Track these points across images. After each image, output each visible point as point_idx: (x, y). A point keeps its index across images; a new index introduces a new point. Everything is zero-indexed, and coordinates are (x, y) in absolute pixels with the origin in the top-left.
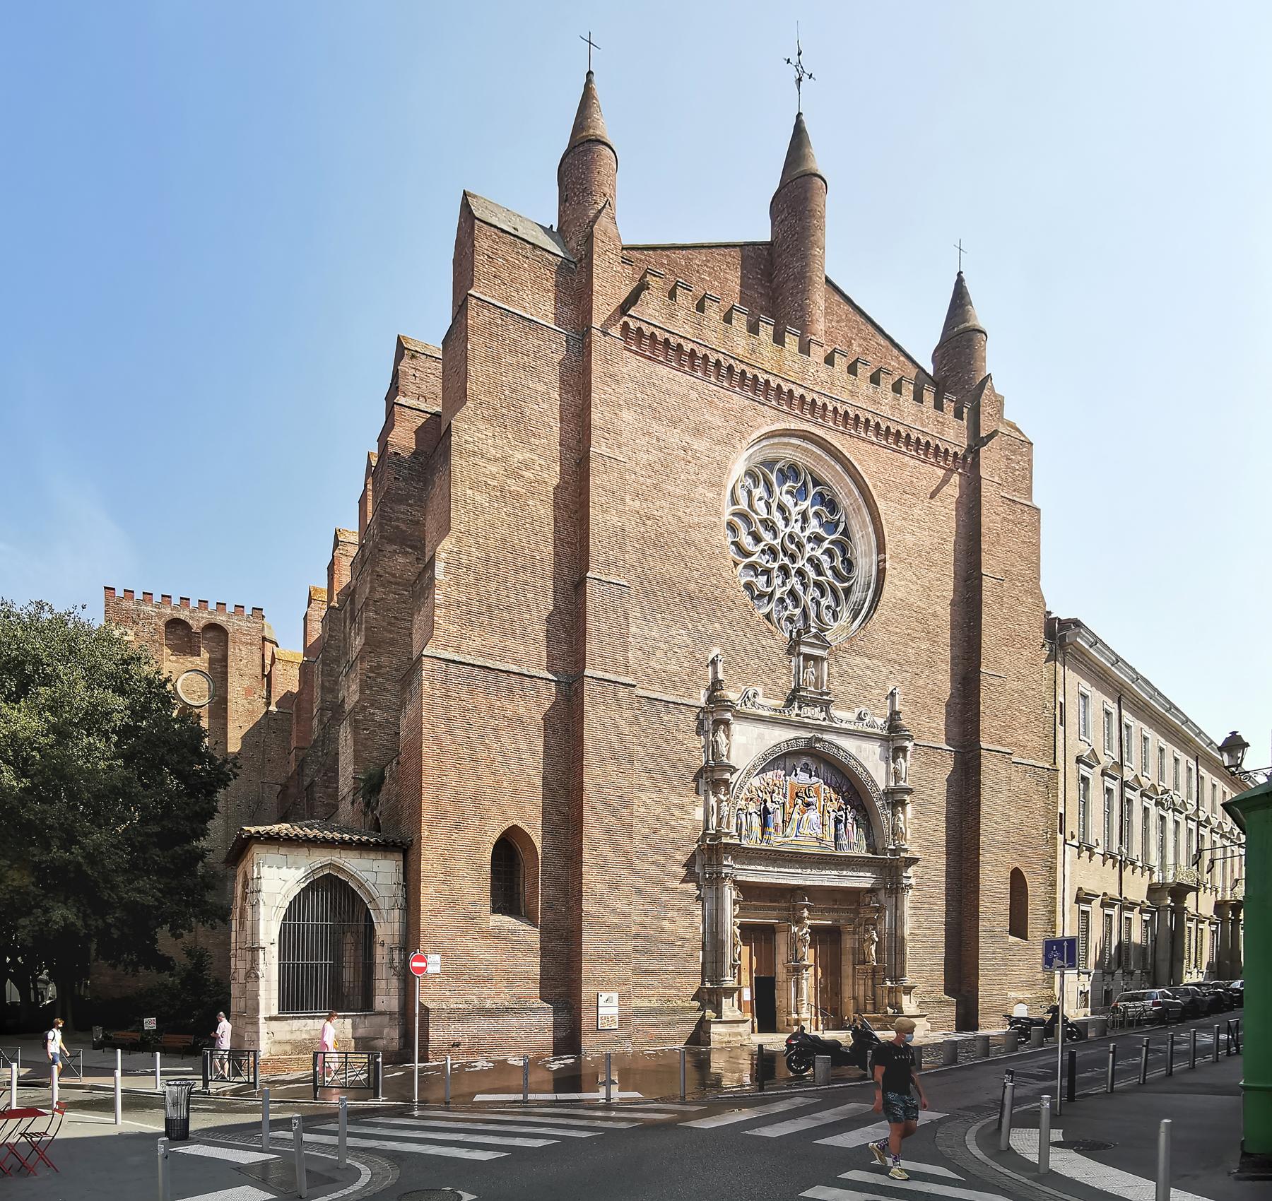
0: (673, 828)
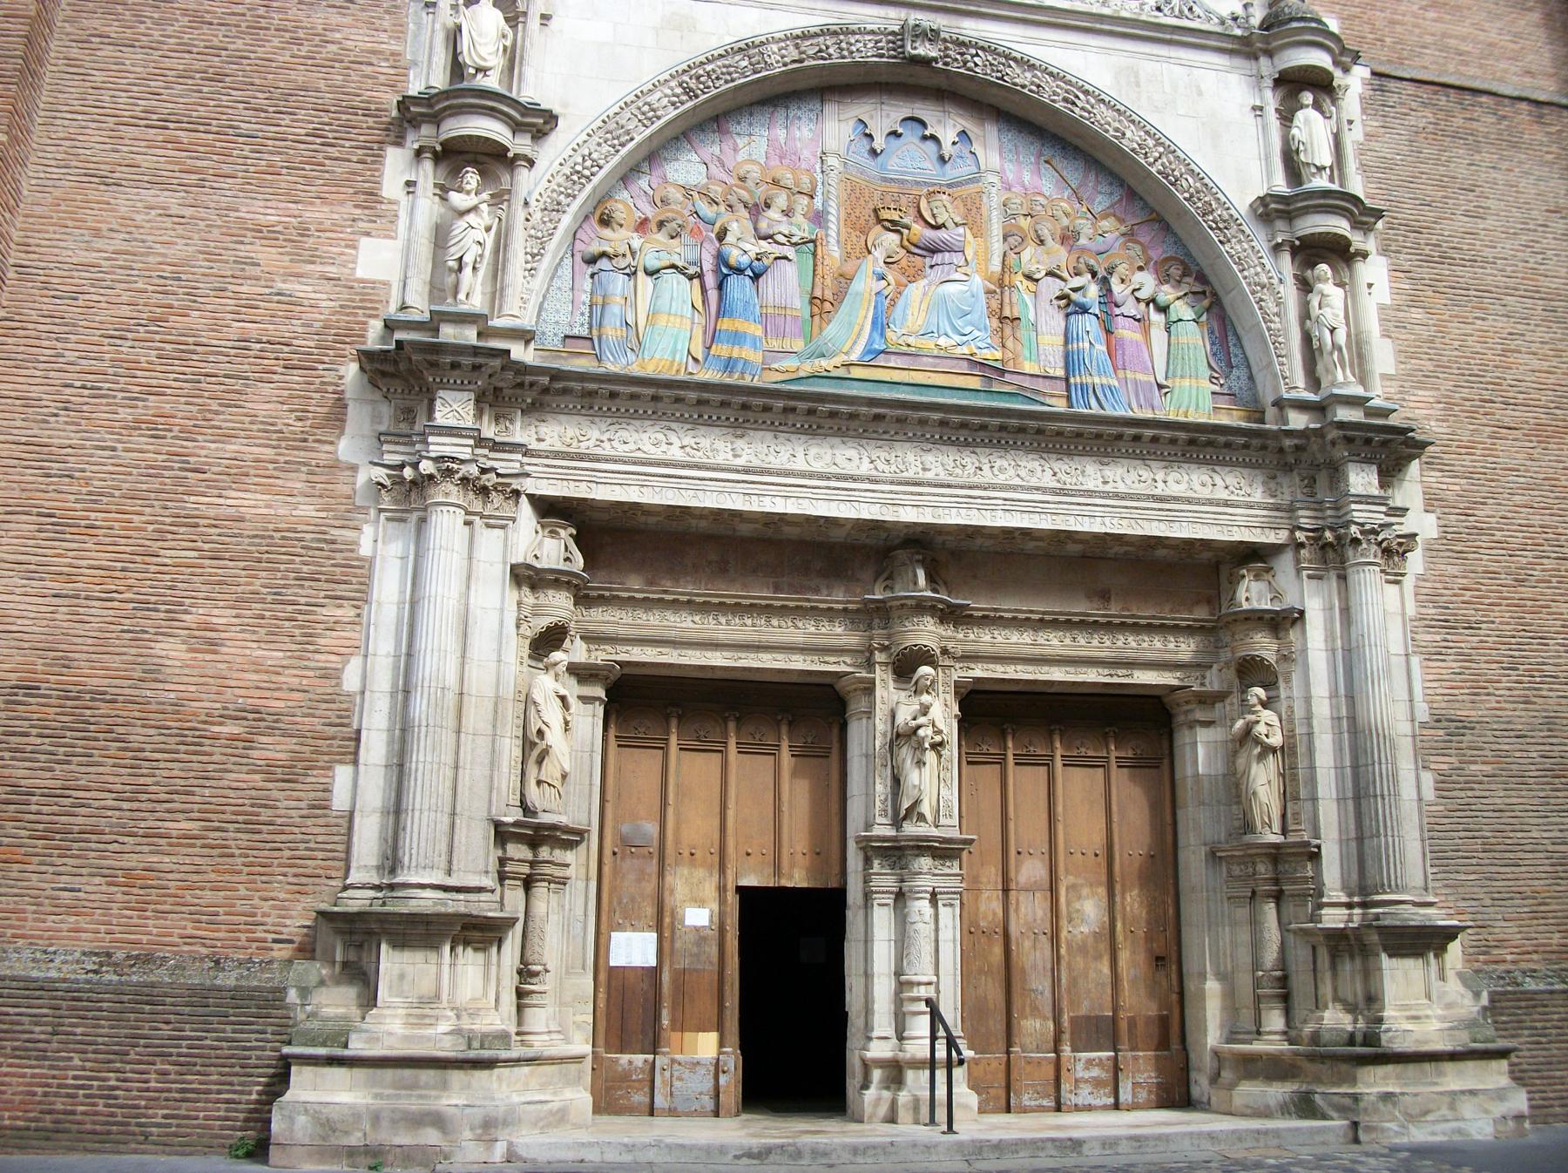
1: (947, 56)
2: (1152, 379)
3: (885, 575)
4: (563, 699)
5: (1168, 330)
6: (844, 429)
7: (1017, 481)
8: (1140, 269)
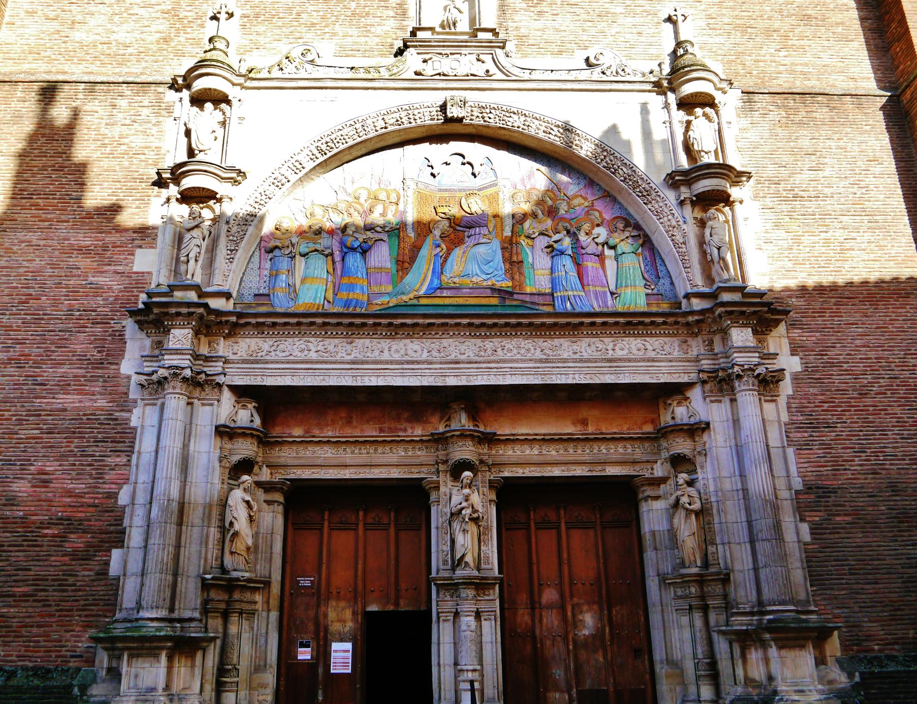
0: (73, 292)
1: (472, 115)
2: (607, 289)
3: (446, 418)
4: (248, 502)
5: (616, 259)
6: (411, 333)
7: (519, 357)
8: (598, 225)
